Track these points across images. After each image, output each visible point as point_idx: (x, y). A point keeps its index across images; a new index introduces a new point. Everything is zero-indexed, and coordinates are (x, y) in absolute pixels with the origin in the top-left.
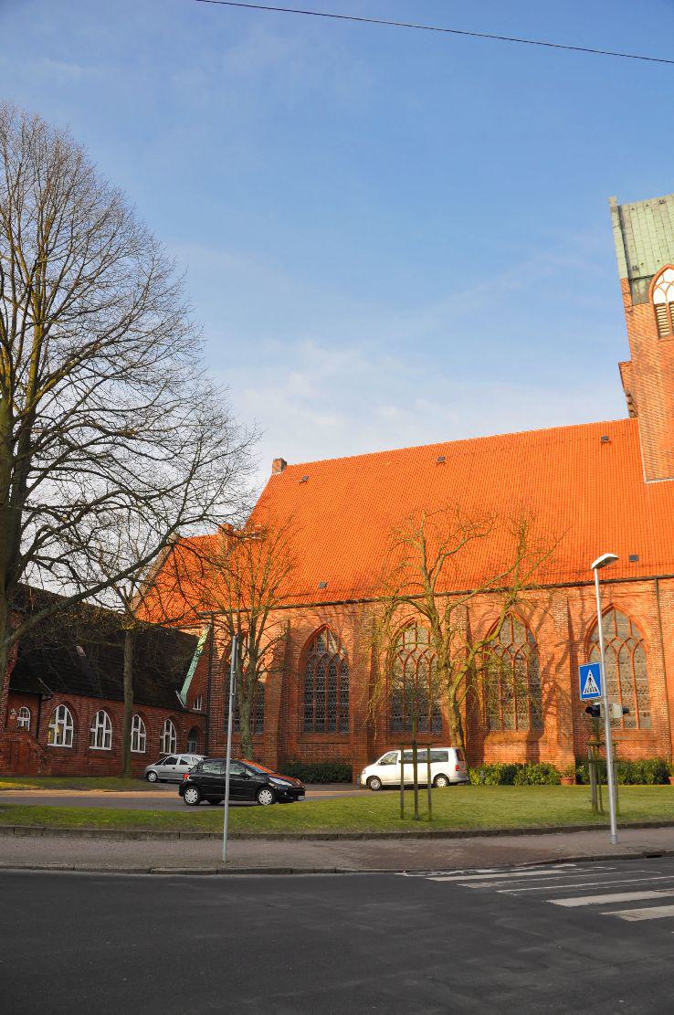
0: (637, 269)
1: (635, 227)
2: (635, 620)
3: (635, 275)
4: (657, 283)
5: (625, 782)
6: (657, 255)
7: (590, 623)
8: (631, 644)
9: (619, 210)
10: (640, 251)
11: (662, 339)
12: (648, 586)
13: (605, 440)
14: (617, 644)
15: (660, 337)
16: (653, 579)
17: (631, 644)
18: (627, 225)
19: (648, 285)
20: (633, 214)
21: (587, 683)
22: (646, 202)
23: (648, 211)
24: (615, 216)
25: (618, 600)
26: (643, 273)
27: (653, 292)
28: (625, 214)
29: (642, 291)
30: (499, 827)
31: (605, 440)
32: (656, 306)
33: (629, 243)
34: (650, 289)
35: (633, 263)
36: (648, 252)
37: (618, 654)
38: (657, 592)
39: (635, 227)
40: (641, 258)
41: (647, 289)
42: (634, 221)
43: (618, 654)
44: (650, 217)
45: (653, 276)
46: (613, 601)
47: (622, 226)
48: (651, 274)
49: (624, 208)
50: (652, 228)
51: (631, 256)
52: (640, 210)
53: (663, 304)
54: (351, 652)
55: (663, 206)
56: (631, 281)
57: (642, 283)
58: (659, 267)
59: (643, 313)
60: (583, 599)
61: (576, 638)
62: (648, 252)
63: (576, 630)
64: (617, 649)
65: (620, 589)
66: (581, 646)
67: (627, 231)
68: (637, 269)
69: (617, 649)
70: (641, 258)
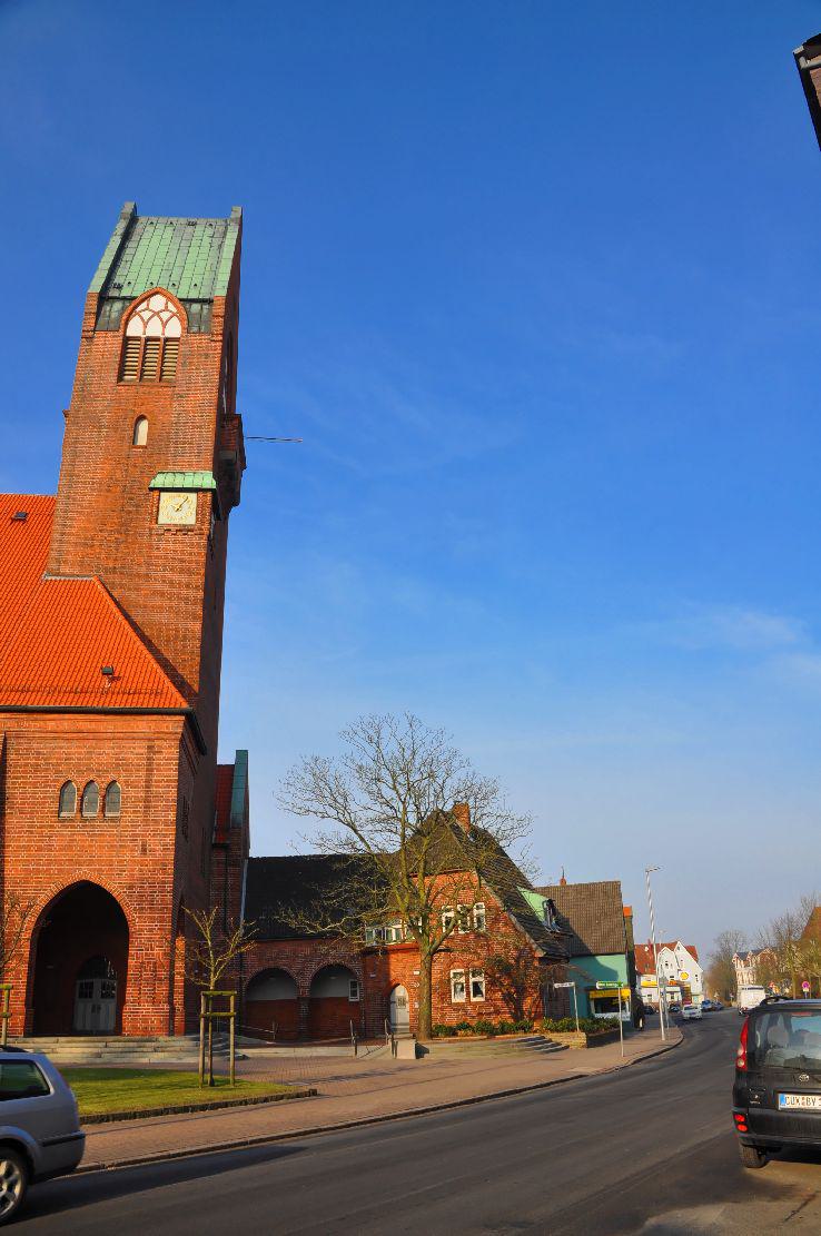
1: (144, 242)
3: (113, 293)
4: (138, 310)
9: (133, 220)
10: (134, 268)
11: (122, 383)
13: (21, 519)
18: (135, 238)
19: (123, 309)
20: (150, 229)
22: (171, 219)
23: (169, 230)
24: (121, 227)
26: (125, 292)
28: (139, 227)
29: (114, 315)
31: (21, 519)
32: (127, 339)
33: (126, 257)
35: (118, 280)
39: (143, 242)
40: (131, 277)
45: (134, 298)
47: (126, 236)
49: (142, 220)
51: (120, 271)
55: (190, 229)
56: (103, 298)
57: (118, 306)
59: (108, 344)
67: (131, 244)
68: (120, 287)
70: (131, 277)
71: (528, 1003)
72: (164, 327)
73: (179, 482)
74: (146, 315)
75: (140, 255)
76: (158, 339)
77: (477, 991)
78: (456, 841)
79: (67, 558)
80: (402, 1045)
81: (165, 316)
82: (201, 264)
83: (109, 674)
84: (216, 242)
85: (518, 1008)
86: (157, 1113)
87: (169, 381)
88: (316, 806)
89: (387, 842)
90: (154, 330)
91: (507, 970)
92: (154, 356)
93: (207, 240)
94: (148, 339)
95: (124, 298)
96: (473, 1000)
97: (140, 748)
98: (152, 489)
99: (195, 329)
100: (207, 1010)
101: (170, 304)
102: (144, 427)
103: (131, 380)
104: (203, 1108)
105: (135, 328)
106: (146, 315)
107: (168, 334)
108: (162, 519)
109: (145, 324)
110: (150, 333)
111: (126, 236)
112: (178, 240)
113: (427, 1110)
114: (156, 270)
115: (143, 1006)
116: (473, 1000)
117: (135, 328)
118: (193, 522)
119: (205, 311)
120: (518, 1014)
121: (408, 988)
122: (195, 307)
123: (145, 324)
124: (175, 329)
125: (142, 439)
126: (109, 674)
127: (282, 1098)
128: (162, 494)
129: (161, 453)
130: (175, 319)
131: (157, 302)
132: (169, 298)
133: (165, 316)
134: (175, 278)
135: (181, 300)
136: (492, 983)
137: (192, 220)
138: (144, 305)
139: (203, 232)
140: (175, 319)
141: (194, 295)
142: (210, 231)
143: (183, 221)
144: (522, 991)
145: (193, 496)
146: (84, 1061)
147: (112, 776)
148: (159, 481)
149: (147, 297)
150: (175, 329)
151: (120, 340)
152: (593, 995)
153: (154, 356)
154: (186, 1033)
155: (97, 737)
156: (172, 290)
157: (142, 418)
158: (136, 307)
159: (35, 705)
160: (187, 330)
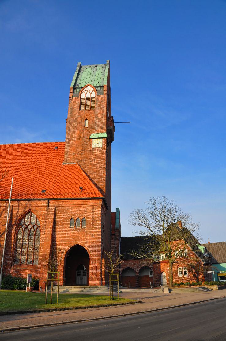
2: (38, 217)
4: (84, 90)
5: (17, 289)
7: (19, 217)
8: (36, 227)
9: (81, 67)
12: (45, 203)
13: (56, 149)
14: (29, 227)
15: (80, 109)
16: (47, 200)
17: (36, 227)
18: (81, 71)
19: (80, 90)
20: (85, 69)
23: (90, 68)
24: (78, 69)
25: (33, 208)
26: (80, 86)
27: (81, 95)
28: (82, 69)
29: (77, 92)
31: (56, 149)
32: (81, 99)
33: (80, 77)
34: (81, 91)
35: (78, 83)
37: (30, 231)
38: (48, 206)
40: (81, 82)
42: (84, 71)
43: (30, 231)
45: (82, 88)
46: (31, 208)
47: (79, 71)
48: (82, 87)
49: (83, 67)
51: (78, 80)
52: (88, 68)
53: (84, 98)
55: (96, 67)
56: (74, 88)
57: (78, 90)
59: (76, 101)
60: (19, 207)
61: (13, 223)
63: (14, 219)
64: (29, 229)
65: (34, 203)
66: (14, 227)
67: (81, 73)
68: (78, 85)
69: (29, 229)
71: (200, 277)
73: (97, 136)
74: (86, 92)
75: (83, 76)
76: (89, 98)
77: (185, 274)
78: (178, 231)
79: (69, 159)
80: (165, 289)
81: (91, 91)
82: (100, 77)
83: (81, 188)
84: (103, 70)
85: (198, 278)
86: (99, 307)
87: (93, 109)
88: (139, 223)
89: (159, 232)
90: (88, 96)
91: (194, 268)
92: (89, 103)
93: (100, 71)
94: (87, 98)
95: (80, 88)
96: (184, 276)
97: (91, 209)
98: (90, 138)
99: (99, 94)
100: (111, 279)
101: (92, 89)
102: (87, 122)
103: (83, 110)
104: (111, 305)
105: (83, 96)
106: (86, 92)
107: (92, 96)
108: (93, 146)
109: (86, 94)
111: (79, 71)
113: (173, 307)
114: (88, 79)
115: (94, 278)
116: (184, 276)
117: (83, 96)
118: (102, 147)
119: (102, 89)
120: (198, 280)
121: (167, 273)
122: (99, 89)
123: (86, 94)
124: (94, 95)
125: (87, 126)
126: (81, 188)
127: (132, 303)
128: (93, 139)
129: (91, 129)
130: (93, 92)
131: (89, 88)
132: (91, 87)
133: (91, 91)
134: (93, 81)
135: (95, 87)
136: (190, 271)
137: (96, 65)
139: (99, 68)
140: (93, 92)
141: (98, 85)
142: (101, 68)
143: (94, 66)
144: (198, 273)
145: (101, 140)
146: (79, 292)
147: (84, 216)
148: (92, 136)
149: (86, 87)
150: (94, 95)
152: (219, 275)
153: (89, 103)
154: (106, 285)
155: (80, 206)
156: (92, 85)
157: (86, 119)
158: (83, 90)
159: (80, 197)
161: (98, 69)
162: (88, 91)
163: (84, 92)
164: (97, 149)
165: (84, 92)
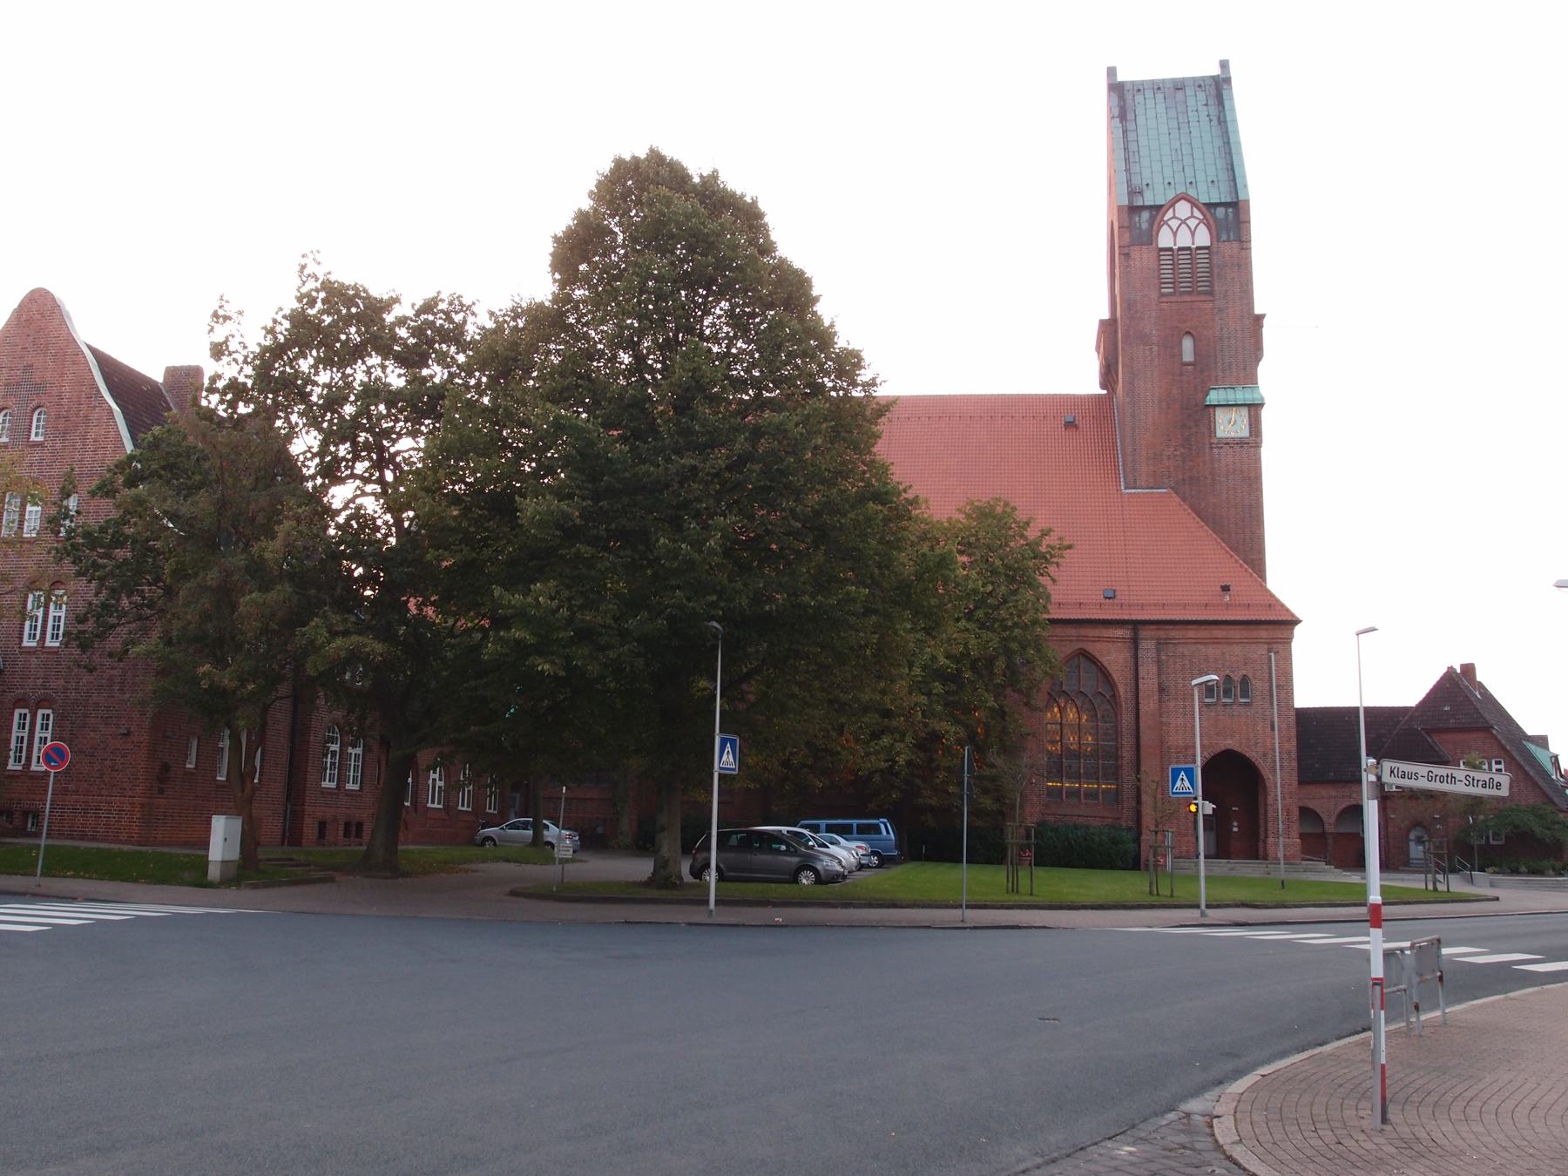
0: (1141, 193)
6: (1168, 172)
10: (1145, 162)
18: (1130, 116)
20: (1139, 98)
21: (1178, 783)
26: (1149, 200)
29: (1145, 226)
30: (1101, 902)
31: (1070, 425)
33: (1132, 147)
36: (1156, 167)
38: (1135, 642)
41: (1151, 224)
44: (1161, 108)
48: (1158, 203)
50: (1164, 129)
51: (1135, 168)
54: (894, 723)
55: (1180, 94)
57: (1145, 215)
58: (1171, 195)
62: (1156, 167)
67: (1131, 126)
70: (1146, 173)
72: (1193, 234)
75: (1143, 141)
82: (1207, 137)
83: (1226, 589)
84: (1213, 110)
90: (1184, 240)
93: (1203, 111)
94: (1180, 249)
95: (1150, 208)
101: (1197, 213)
105: (1165, 239)
106: (1174, 224)
109: (1175, 234)
110: (1180, 244)
112: (1172, 113)
114: (1167, 161)
117: (1165, 239)
122: (1220, 212)
123: (1175, 234)
124: (1203, 238)
131: (1183, 209)
132: (1194, 203)
133: (1192, 223)
138: (1171, 211)
142: (1201, 96)
149: (1172, 204)
150: (1203, 238)
151: (1154, 254)
155: (1228, 642)
156: (1192, 192)
160: (1216, 237)
161: (1191, 102)
162: (1184, 222)
163: (1166, 223)
164: (1229, 443)
165: (1166, 223)
